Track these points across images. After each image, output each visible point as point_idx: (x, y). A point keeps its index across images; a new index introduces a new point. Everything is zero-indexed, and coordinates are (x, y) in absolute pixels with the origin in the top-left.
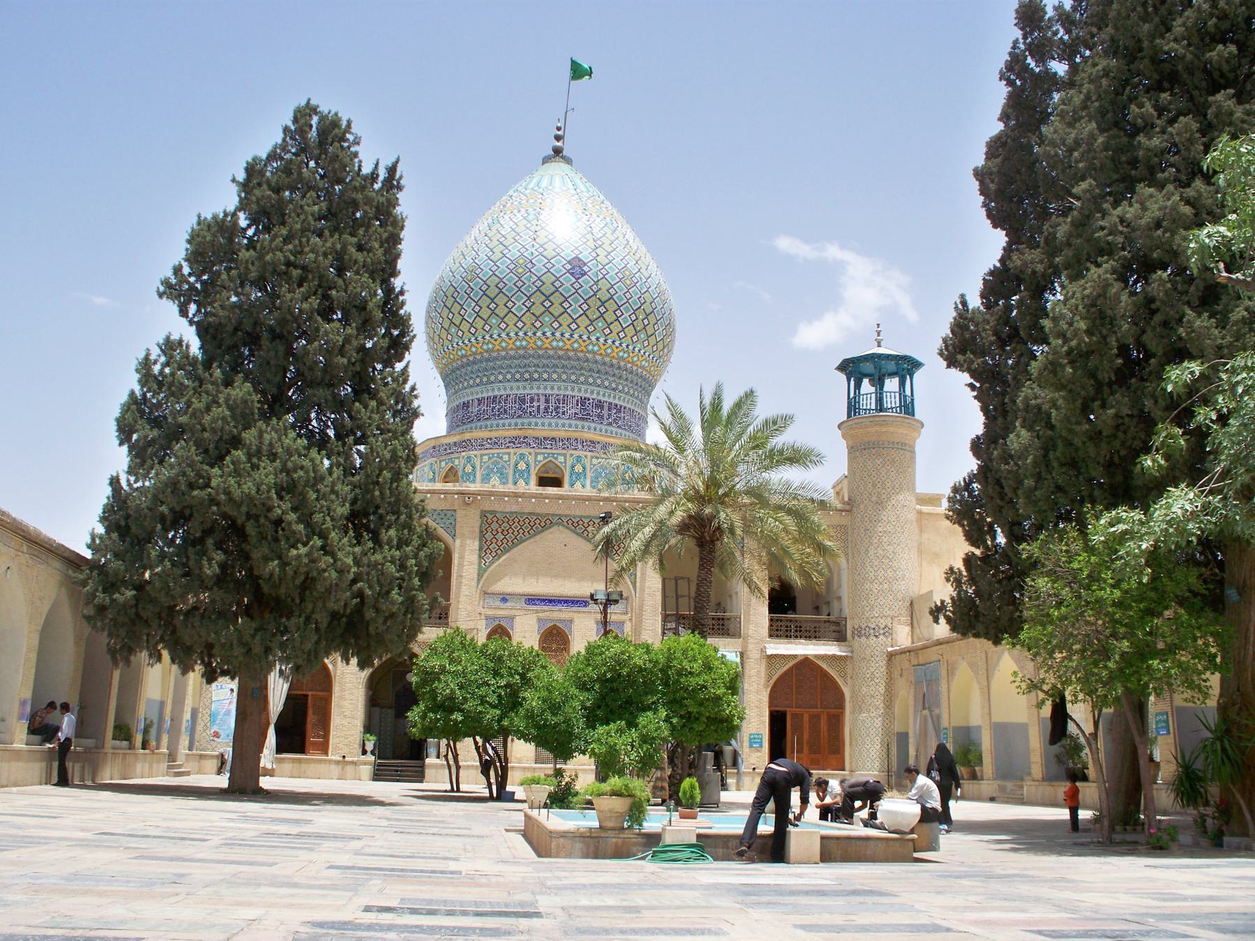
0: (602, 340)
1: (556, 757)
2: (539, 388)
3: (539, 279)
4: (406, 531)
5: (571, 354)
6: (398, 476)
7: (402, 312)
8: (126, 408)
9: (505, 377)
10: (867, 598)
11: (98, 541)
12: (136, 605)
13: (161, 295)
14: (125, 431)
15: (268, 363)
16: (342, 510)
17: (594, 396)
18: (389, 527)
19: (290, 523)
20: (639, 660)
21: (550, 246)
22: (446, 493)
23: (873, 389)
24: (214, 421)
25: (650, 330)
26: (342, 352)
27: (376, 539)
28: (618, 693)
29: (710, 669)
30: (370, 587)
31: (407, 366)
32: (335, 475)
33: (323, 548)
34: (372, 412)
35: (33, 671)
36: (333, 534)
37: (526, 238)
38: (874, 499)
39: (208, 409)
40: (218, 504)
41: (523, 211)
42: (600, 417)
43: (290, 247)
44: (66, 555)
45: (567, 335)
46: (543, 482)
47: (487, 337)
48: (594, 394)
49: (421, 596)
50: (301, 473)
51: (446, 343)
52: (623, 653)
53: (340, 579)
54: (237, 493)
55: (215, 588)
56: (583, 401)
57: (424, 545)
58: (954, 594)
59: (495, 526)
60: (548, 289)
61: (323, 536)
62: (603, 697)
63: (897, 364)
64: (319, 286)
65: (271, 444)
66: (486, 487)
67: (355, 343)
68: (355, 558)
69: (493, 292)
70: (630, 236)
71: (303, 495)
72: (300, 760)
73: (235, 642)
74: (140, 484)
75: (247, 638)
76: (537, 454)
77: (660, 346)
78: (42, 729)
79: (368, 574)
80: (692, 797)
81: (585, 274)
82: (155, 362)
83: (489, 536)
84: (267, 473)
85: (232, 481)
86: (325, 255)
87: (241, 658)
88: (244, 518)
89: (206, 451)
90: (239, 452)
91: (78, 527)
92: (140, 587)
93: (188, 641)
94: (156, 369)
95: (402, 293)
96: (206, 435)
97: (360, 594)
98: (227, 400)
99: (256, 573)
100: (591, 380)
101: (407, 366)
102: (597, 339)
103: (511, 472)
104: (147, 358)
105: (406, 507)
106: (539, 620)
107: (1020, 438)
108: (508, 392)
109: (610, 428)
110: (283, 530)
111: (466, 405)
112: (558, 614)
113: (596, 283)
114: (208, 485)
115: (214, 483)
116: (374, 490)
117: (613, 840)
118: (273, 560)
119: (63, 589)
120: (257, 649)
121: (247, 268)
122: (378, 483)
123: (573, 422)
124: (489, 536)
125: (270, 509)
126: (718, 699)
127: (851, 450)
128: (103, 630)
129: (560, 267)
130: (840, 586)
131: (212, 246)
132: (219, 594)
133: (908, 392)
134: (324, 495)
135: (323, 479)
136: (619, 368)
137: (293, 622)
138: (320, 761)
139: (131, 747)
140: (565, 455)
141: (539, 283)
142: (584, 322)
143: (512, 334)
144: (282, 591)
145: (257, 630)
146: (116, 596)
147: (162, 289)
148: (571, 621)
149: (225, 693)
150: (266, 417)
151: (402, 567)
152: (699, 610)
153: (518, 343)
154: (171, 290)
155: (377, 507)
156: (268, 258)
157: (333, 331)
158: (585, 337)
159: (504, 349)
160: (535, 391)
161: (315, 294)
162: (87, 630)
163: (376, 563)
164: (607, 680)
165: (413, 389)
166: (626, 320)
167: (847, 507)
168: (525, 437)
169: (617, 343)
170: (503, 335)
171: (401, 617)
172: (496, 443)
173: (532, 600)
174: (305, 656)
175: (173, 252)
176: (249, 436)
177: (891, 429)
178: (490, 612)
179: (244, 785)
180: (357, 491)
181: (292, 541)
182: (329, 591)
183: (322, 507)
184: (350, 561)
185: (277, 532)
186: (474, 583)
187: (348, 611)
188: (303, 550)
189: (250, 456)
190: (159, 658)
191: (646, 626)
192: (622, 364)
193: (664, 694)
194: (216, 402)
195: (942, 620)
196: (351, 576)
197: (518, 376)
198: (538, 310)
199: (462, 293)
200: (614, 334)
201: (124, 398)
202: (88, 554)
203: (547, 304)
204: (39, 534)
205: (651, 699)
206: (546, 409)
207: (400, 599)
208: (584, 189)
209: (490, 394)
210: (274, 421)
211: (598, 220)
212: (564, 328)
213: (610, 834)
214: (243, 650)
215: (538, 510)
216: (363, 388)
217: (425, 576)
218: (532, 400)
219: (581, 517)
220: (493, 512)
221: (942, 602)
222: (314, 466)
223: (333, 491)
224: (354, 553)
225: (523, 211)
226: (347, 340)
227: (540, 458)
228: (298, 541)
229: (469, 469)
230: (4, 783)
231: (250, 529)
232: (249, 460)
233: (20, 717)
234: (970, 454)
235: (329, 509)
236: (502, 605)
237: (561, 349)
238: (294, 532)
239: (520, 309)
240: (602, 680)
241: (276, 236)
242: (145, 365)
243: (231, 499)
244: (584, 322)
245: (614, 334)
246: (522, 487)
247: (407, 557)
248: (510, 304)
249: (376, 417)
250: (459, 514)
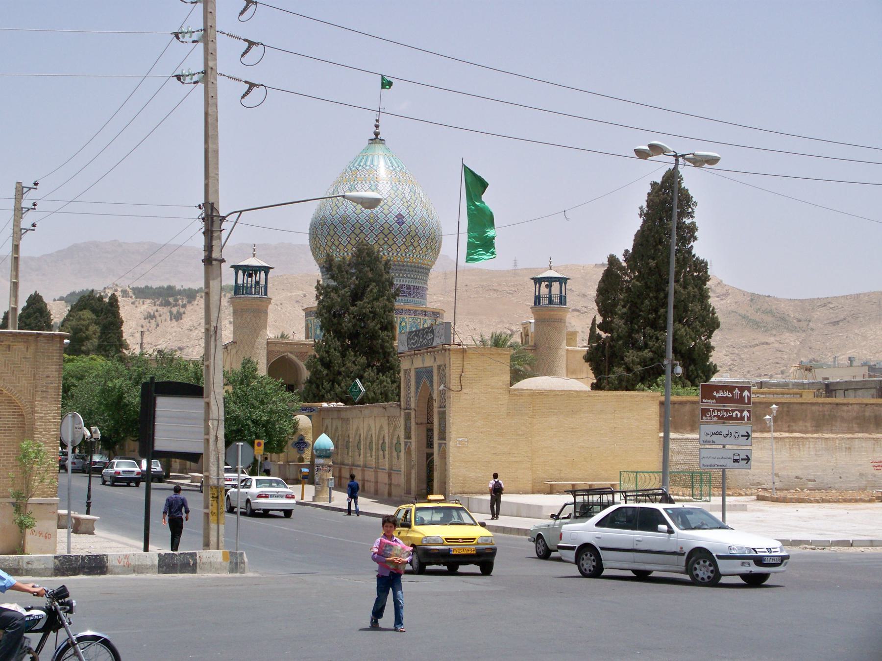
42: (410, 294)
60: (386, 232)
129: (392, 219)
133: (563, 293)
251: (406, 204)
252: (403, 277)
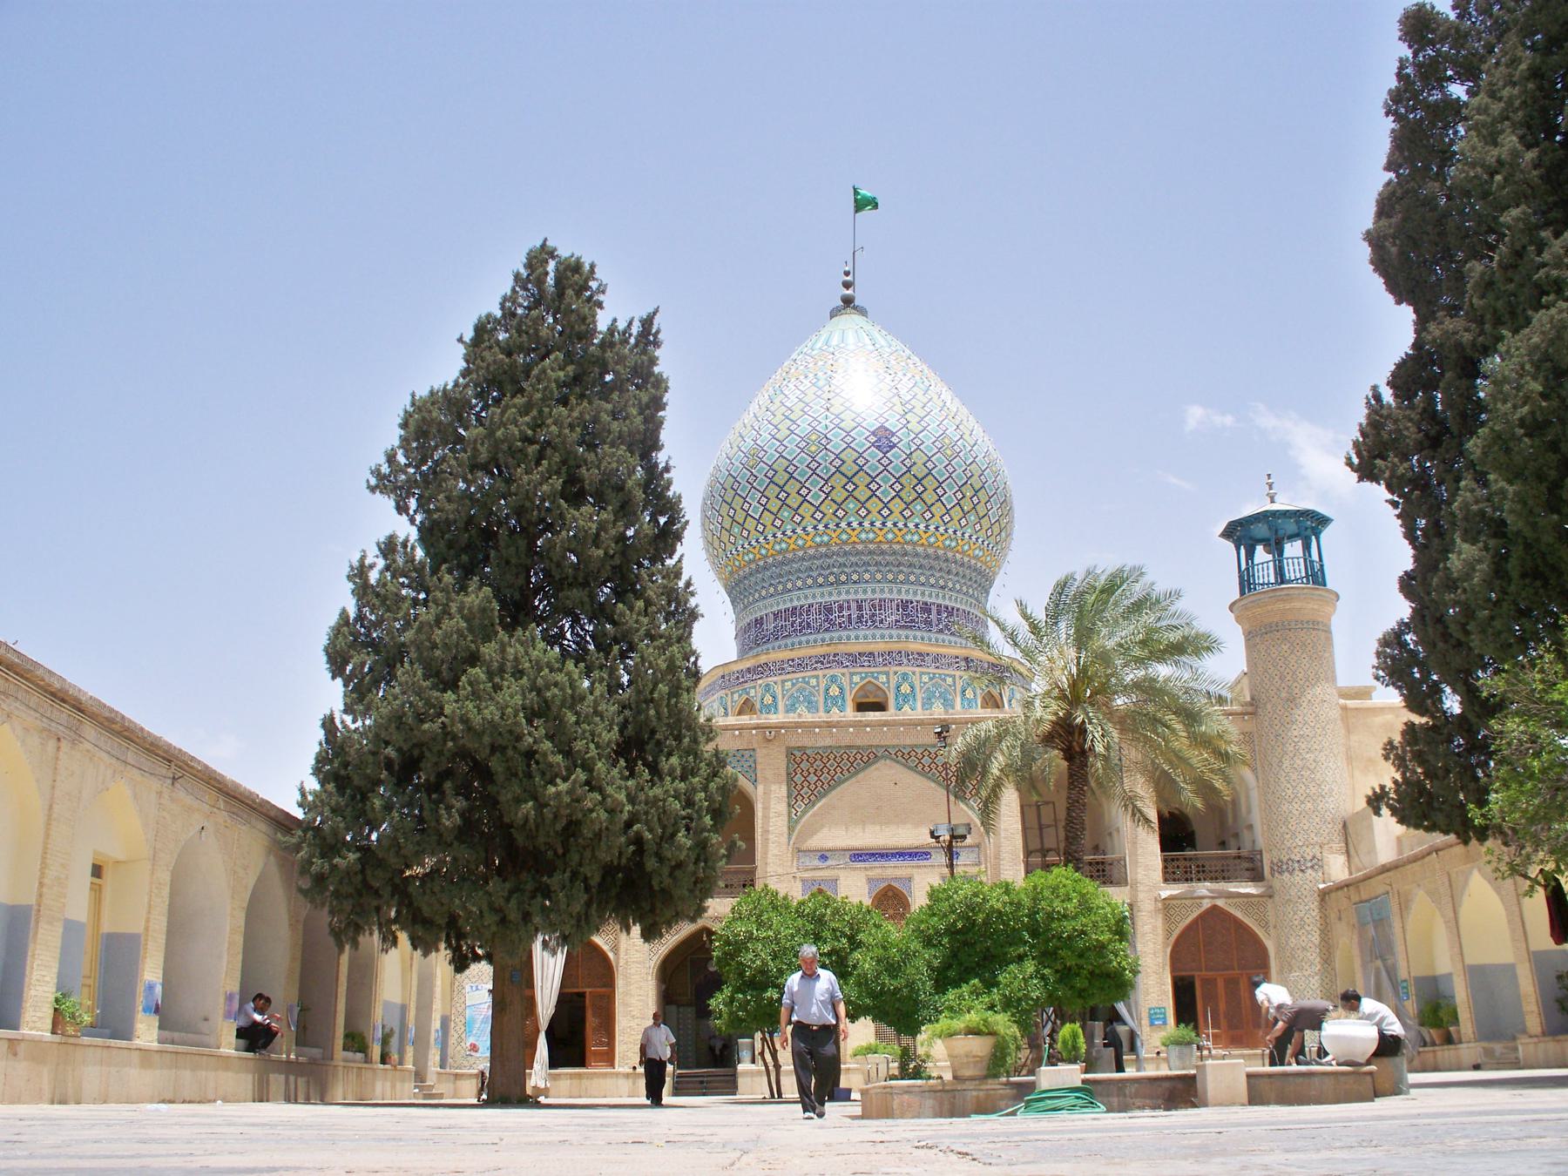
0: (922, 526)
1: (899, 1032)
2: (848, 592)
3: (837, 457)
4: (691, 758)
5: (885, 547)
6: (676, 690)
7: (670, 494)
8: (337, 631)
9: (804, 582)
10: (1286, 823)
11: (310, 798)
12: (363, 871)
13: (372, 489)
14: (337, 661)
15: (508, 562)
16: (611, 736)
17: (919, 598)
18: (670, 754)
19: (545, 755)
20: (997, 902)
21: (847, 416)
22: (741, 728)
23: (1270, 557)
24: (447, 635)
25: (981, 510)
26: (596, 541)
27: (654, 769)
28: (972, 947)
29: (1090, 909)
30: (651, 830)
31: (680, 561)
32: (597, 693)
33: (587, 783)
34: (639, 614)
35: (240, 957)
36: (600, 765)
37: (817, 408)
38: (1284, 695)
39: (438, 622)
40: (454, 738)
41: (811, 376)
42: (928, 623)
43: (527, 419)
44: (272, 814)
45: (878, 524)
46: (861, 707)
47: (779, 535)
48: (917, 595)
49: (715, 839)
50: (556, 691)
51: (729, 547)
52: (976, 895)
53: (611, 821)
54: (477, 720)
55: (456, 844)
56: (905, 605)
57: (715, 774)
58: (1398, 777)
59: (804, 765)
60: (849, 469)
61: (588, 767)
62: (954, 955)
63: (1297, 522)
64: (564, 462)
65: (516, 659)
66: (792, 718)
67: (613, 532)
68: (628, 795)
69: (781, 478)
70: (947, 395)
71: (560, 718)
72: (579, 1076)
73: (485, 908)
74: (359, 723)
75: (500, 902)
76: (852, 674)
77: (996, 529)
78: (255, 1038)
79: (646, 813)
80: (1075, 1048)
81: (895, 446)
82: (372, 566)
83: (798, 778)
84: (513, 694)
85: (470, 705)
86: (572, 427)
87: (494, 928)
88: (488, 751)
89: (438, 674)
90: (477, 669)
91: (287, 780)
92: (366, 851)
93: (426, 911)
94: (373, 576)
95: (667, 469)
96: (438, 653)
97: (638, 841)
98: (460, 610)
99: (506, 820)
100: (912, 578)
101: (680, 561)
102: (917, 526)
103: (821, 700)
104: (362, 564)
105: (689, 728)
106: (870, 880)
107: (1464, 554)
108: (810, 601)
109: (941, 636)
110: (537, 763)
111: (759, 622)
112: (892, 870)
113: (909, 456)
114: (441, 714)
115: (447, 710)
116: (648, 709)
117: (973, 1093)
118: (526, 802)
119: (272, 858)
120: (514, 915)
121: (475, 449)
122: (652, 700)
123: (894, 632)
124: (798, 778)
125: (519, 738)
126: (1102, 947)
127: (1250, 636)
128: (323, 905)
129: (862, 440)
130: (1249, 811)
131: (428, 425)
132: (465, 853)
133: (1315, 557)
134: (587, 716)
135: (583, 698)
136: (947, 560)
137: (554, 881)
138: (605, 1075)
139: (368, 1060)
140: (887, 674)
141: (837, 463)
142: (897, 505)
143: (809, 529)
144: (541, 840)
145: (511, 892)
146: (337, 860)
147: (373, 481)
148: (910, 879)
149: (481, 976)
150: (510, 629)
151: (689, 803)
152: (1070, 834)
153: (818, 539)
154: (382, 483)
155: (653, 732)
156: (499, 433)
157: (586, 517)
158: (900, 525)
160: (844, 597)
161: (558, 473)
162: (305, 908)
163: (656, 799)
164: (958, 932)
165: (688, 584)
166: (950, 498)
167: (1250, 709)
169: (941, 529)
170: (799, 530)
171: (691, 867)
172: (800, 665)
173: (860, 855)
174: (573, 922)
175: (385, 436)
176: (488, 650)
177: (1297, 605)
178: (806, 875)
179: (504, 1089)
180: (627, 712)
181: (548, 777)
182: (598, 836)
183: (584, 732)
184: (622, 797)
185: (529, 766)
186: (784, 839)
187: (624, 861)
188: (563, 787)
189: (490, 675)
190: (395, 942)
191: (1002, 861)
192: (950, 555)
193: (1032, 946)
194: (446, 612)
195: (1385, 811)
196: (625, 816)
197: (821, 580)
198: (839, 495)
199: (744, 483)
200: (937, 518)
201: (333, 619)
202: (299, 814)
203: (850, 487)
204: (237, 786)
205: (1013, 952)
206: (860, 617)
207: (689, 843)
208: (883, 343)
209: (789, 605)
210: (519, 631)
211: (905, 379)
212: (874, 516)
213: (969, 1085)
214: (496, 918)
215: (859, 742)
216: (626, 588)
217: (718, 814)
218: (841, 608)
219: (913, 747)
220: (802, 749)
221: (1382, 787)
222: (573, 686)
223: (596, 713)
224: (627, 788)
225: (811, 376)
226: (602, 526)
227: (856, 679)
228: (556, 776)
229: (768, 699)
230: (211, 1097)
231: (495, 764)
232: (491, 679)
233: (228, 1015)
234: (1401, 596)
235: (593, 735)
236: (821, 865)
237: (871, 542)
238: (551, 765)
239: (816, 496)
240: (951, 931)
241: (507, 407)
242: (359, 573)
243: (470, 729)
244: (897, 505)
245: (937, 518)
246: (835, 715)
247: (694, 790)
248: (804, 492)
249: (645, 620)
250: (760, 754)
251: (899, 408)
252: (906, 582)
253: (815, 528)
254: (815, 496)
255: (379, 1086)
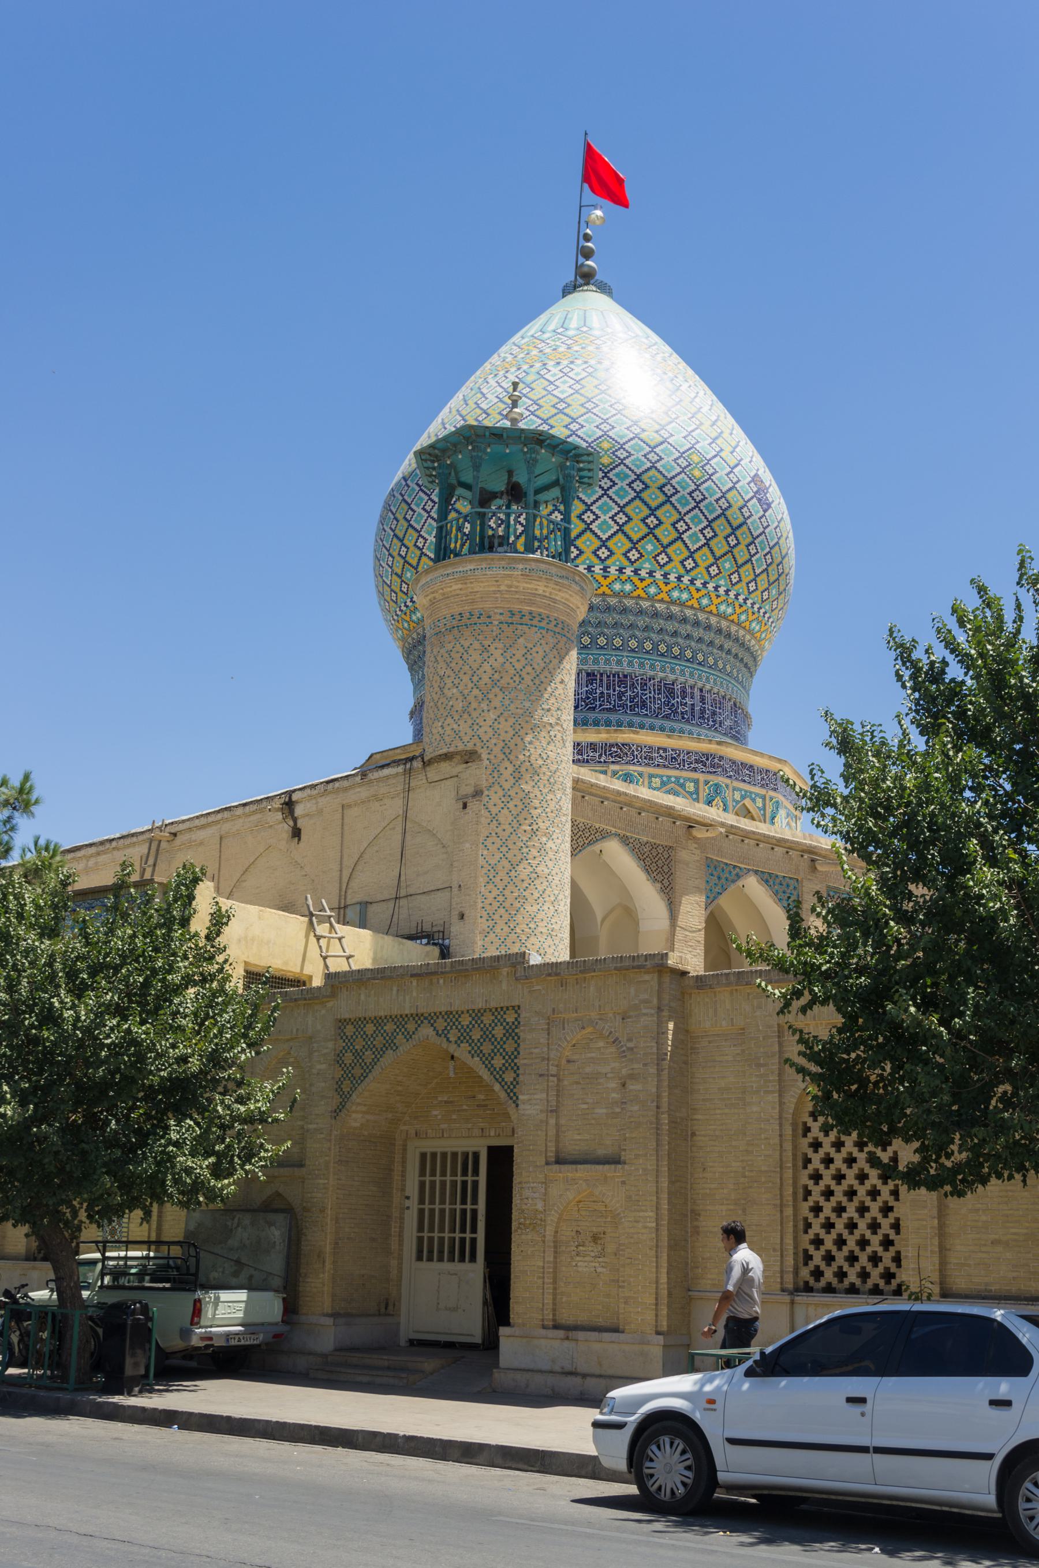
47: (628, 571)
141: (723, 503)
143: (672, 577)
153: (675, 594)
159: (650, 598)
168: (721, 758)
170: (658, 575)
206: (703, 711)
218: (684, 691)
239: (694, 538)
253: (679, 578)
254: (694, 538)
255: (129, 1361)
